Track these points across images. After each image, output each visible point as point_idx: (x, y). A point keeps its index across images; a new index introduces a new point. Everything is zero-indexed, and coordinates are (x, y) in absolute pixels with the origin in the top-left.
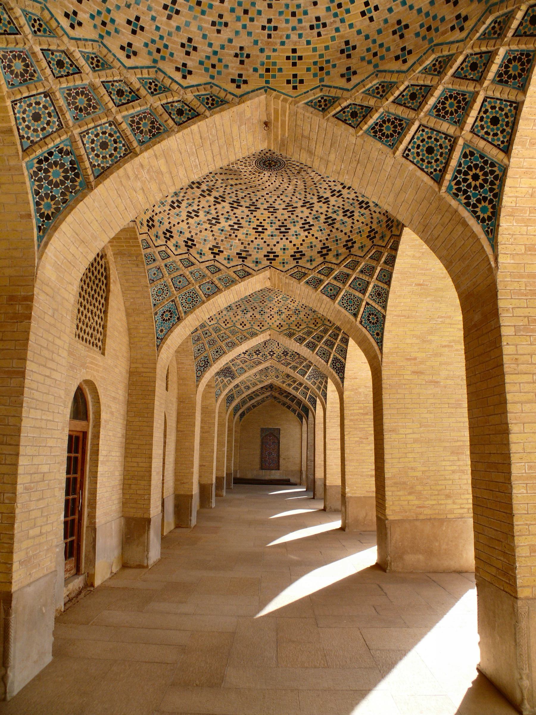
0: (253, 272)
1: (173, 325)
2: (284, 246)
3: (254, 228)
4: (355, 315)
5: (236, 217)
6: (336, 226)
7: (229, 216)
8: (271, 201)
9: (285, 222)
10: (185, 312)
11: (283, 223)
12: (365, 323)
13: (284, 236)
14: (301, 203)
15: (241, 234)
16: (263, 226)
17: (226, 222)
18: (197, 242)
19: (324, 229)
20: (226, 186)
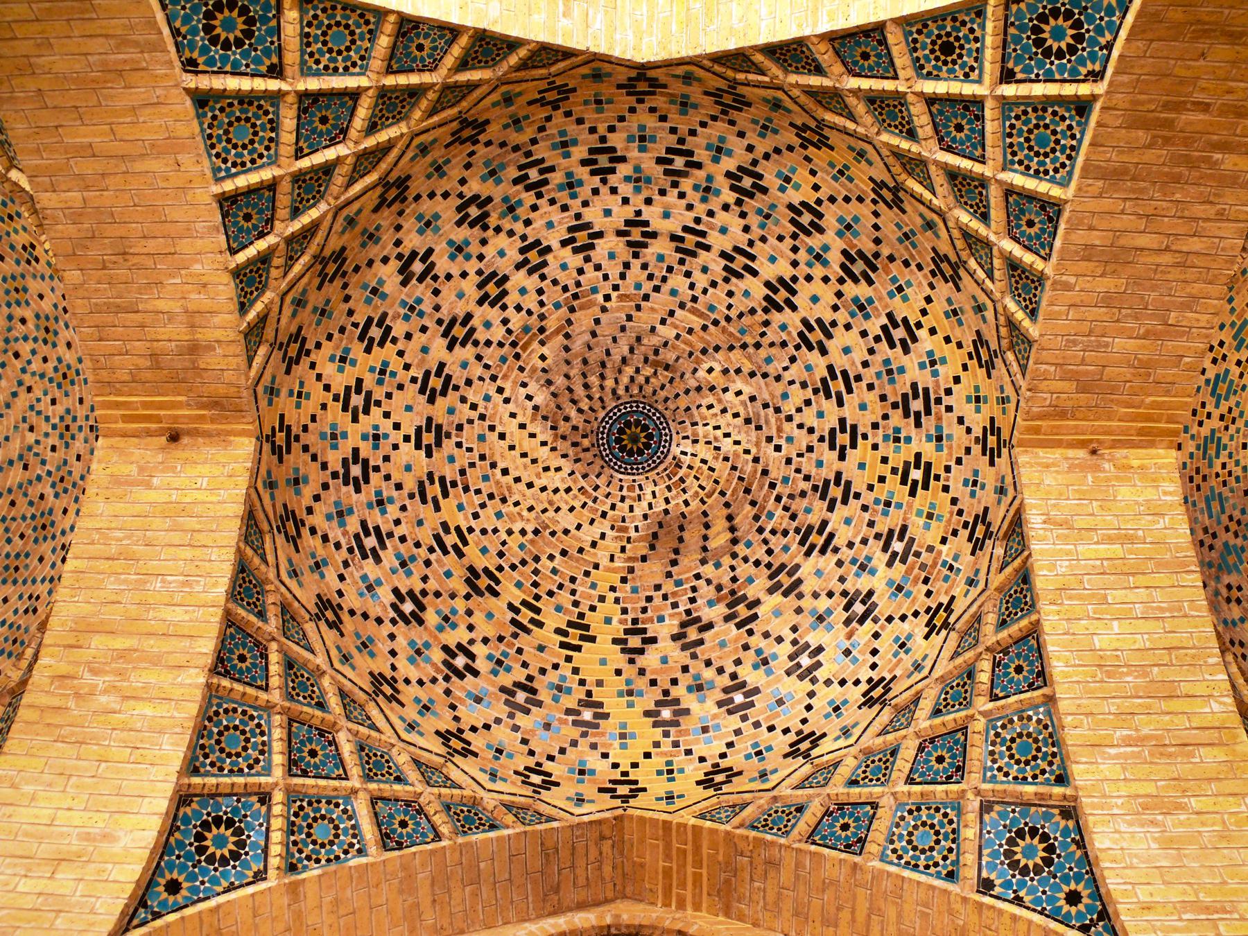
0: (1017, 503)
1: (1081, 844)
2: (969, 399)
3: (913, 493)
4: (1082, 107)
5: (864, 541)
6: (868, 247)
7: (854, 561)
8: (803, 439)
9: (891, 399)
10: (1061, 780)
11: (895, 406)
12: (1093, 57)
13: (938, 401)
14: (814, 357)
15: (925, 534)
16: (907, 464)
17: (873, 572)
18: (890, 671)
19: (894, 280)
20: (734, 556)
